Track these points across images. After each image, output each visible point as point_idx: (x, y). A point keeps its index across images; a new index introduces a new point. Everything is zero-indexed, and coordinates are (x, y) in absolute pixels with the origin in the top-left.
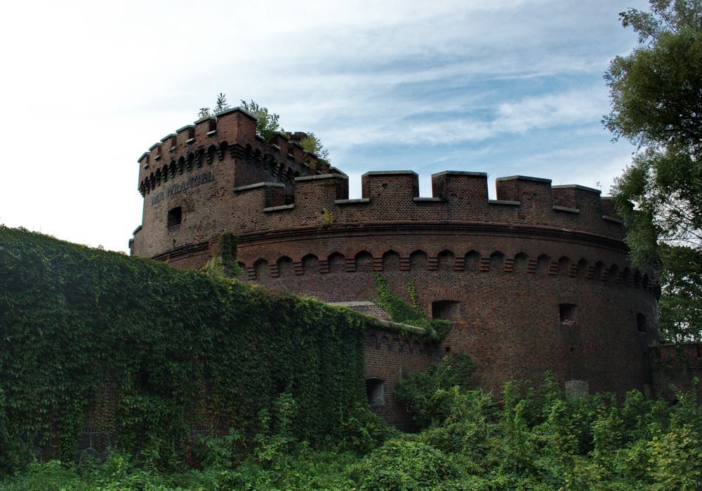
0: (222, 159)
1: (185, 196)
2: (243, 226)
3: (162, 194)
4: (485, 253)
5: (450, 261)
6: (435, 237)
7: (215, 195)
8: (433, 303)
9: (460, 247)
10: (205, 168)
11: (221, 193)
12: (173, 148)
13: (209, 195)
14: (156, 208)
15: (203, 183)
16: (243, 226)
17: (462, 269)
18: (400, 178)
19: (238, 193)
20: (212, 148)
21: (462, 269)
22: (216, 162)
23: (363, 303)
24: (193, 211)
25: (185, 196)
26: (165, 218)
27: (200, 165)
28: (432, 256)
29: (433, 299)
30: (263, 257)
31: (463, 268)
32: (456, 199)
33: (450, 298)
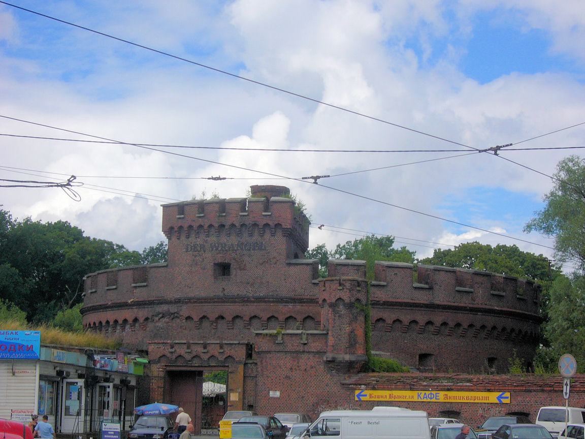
0: (273, 235)
1: (233, 255)
2: (294, 291)
3: (202, 247)
4: (452, 324)
5: (431, 328)
6: (424, 312)
7: (267, 262)
8: (419, 355)
9: (438, 318)
10: (256, 237)
11: (275, 260)
12: (224, 214)
13: (261, 261)
14: (193, 255)
15: (254, 249)
16: (294, 291)
17: (437, 333)
18: (405, 270)
19: (290, 264)
20: (267, 225)
21: (437, 333)
22: (267, 236)
23: (378, 353)
24: (244, 270)
25: (233, 255)
26: (210, 267)
27: (251, 235)
28: (422, 325)
29: (419, 352)
30: (311, 315)
31: (438, 333)
32: (438, 287)
33: (429, 352)
